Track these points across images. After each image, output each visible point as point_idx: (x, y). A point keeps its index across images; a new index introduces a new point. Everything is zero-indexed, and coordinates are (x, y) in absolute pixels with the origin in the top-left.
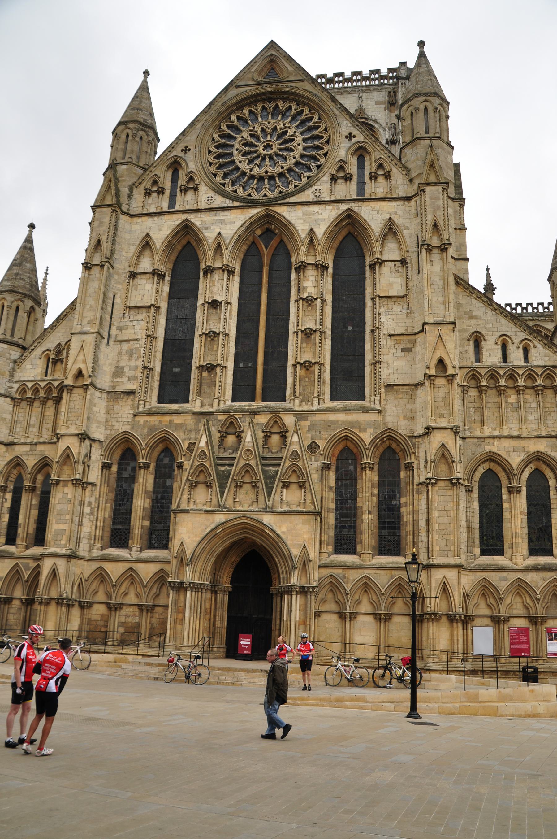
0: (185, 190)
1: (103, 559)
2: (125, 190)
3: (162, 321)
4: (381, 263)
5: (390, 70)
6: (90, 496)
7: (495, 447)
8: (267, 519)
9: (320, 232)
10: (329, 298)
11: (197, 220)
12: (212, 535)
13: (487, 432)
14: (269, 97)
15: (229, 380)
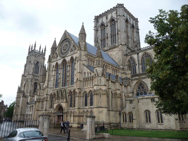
0: (57, 57)
1: (49, 110)
2: (51, 59)
3: (56, 77)
4: (75, 64)
5: (116, 6)
6: (48, 102)
7: (86, 90)
8: (62, 103)
9: (69, 60)
10: (71, 70)
11: (58, 62)
12: (57, 106)
13: (85, 88)
14: (66, 39)
15: (61, 84)
